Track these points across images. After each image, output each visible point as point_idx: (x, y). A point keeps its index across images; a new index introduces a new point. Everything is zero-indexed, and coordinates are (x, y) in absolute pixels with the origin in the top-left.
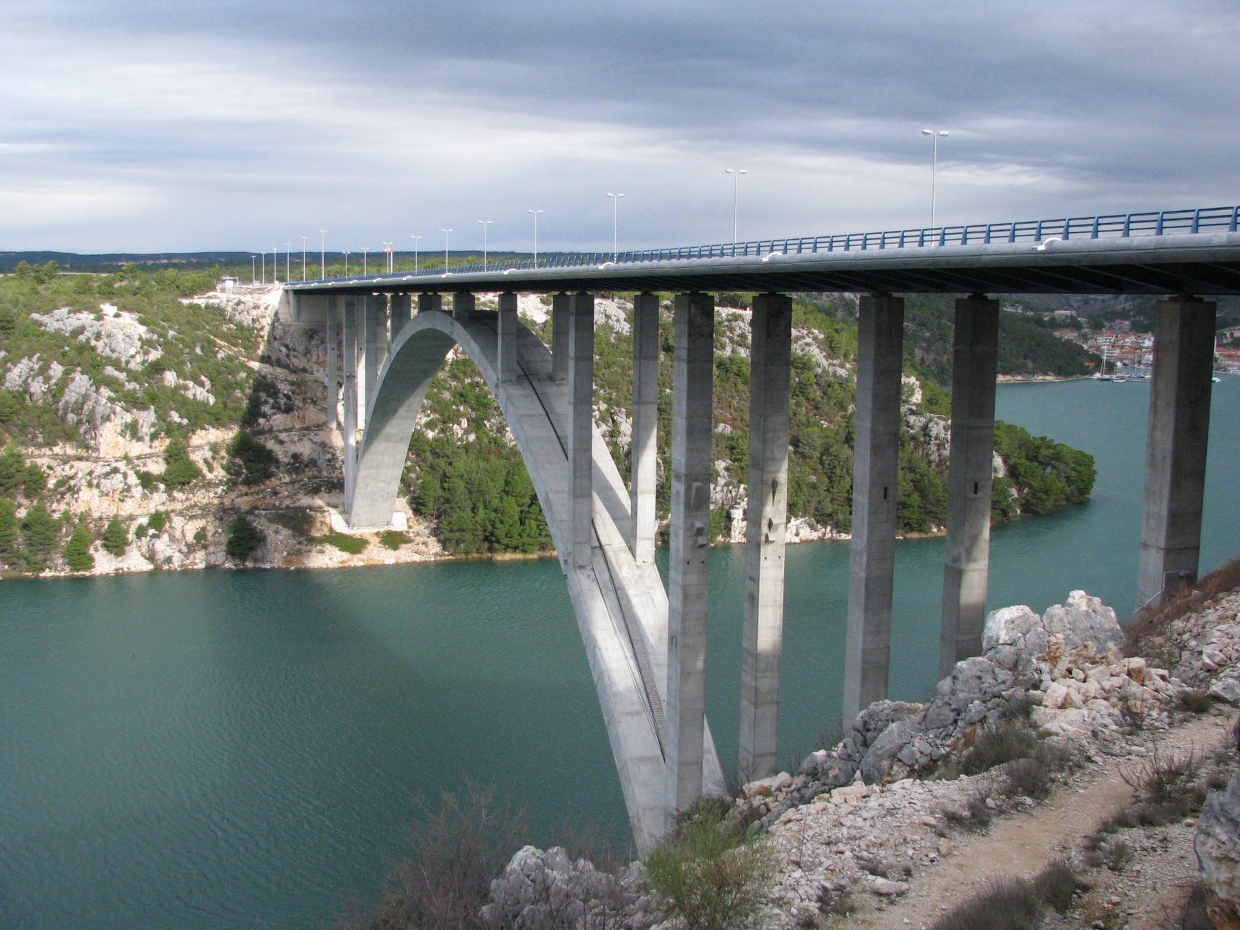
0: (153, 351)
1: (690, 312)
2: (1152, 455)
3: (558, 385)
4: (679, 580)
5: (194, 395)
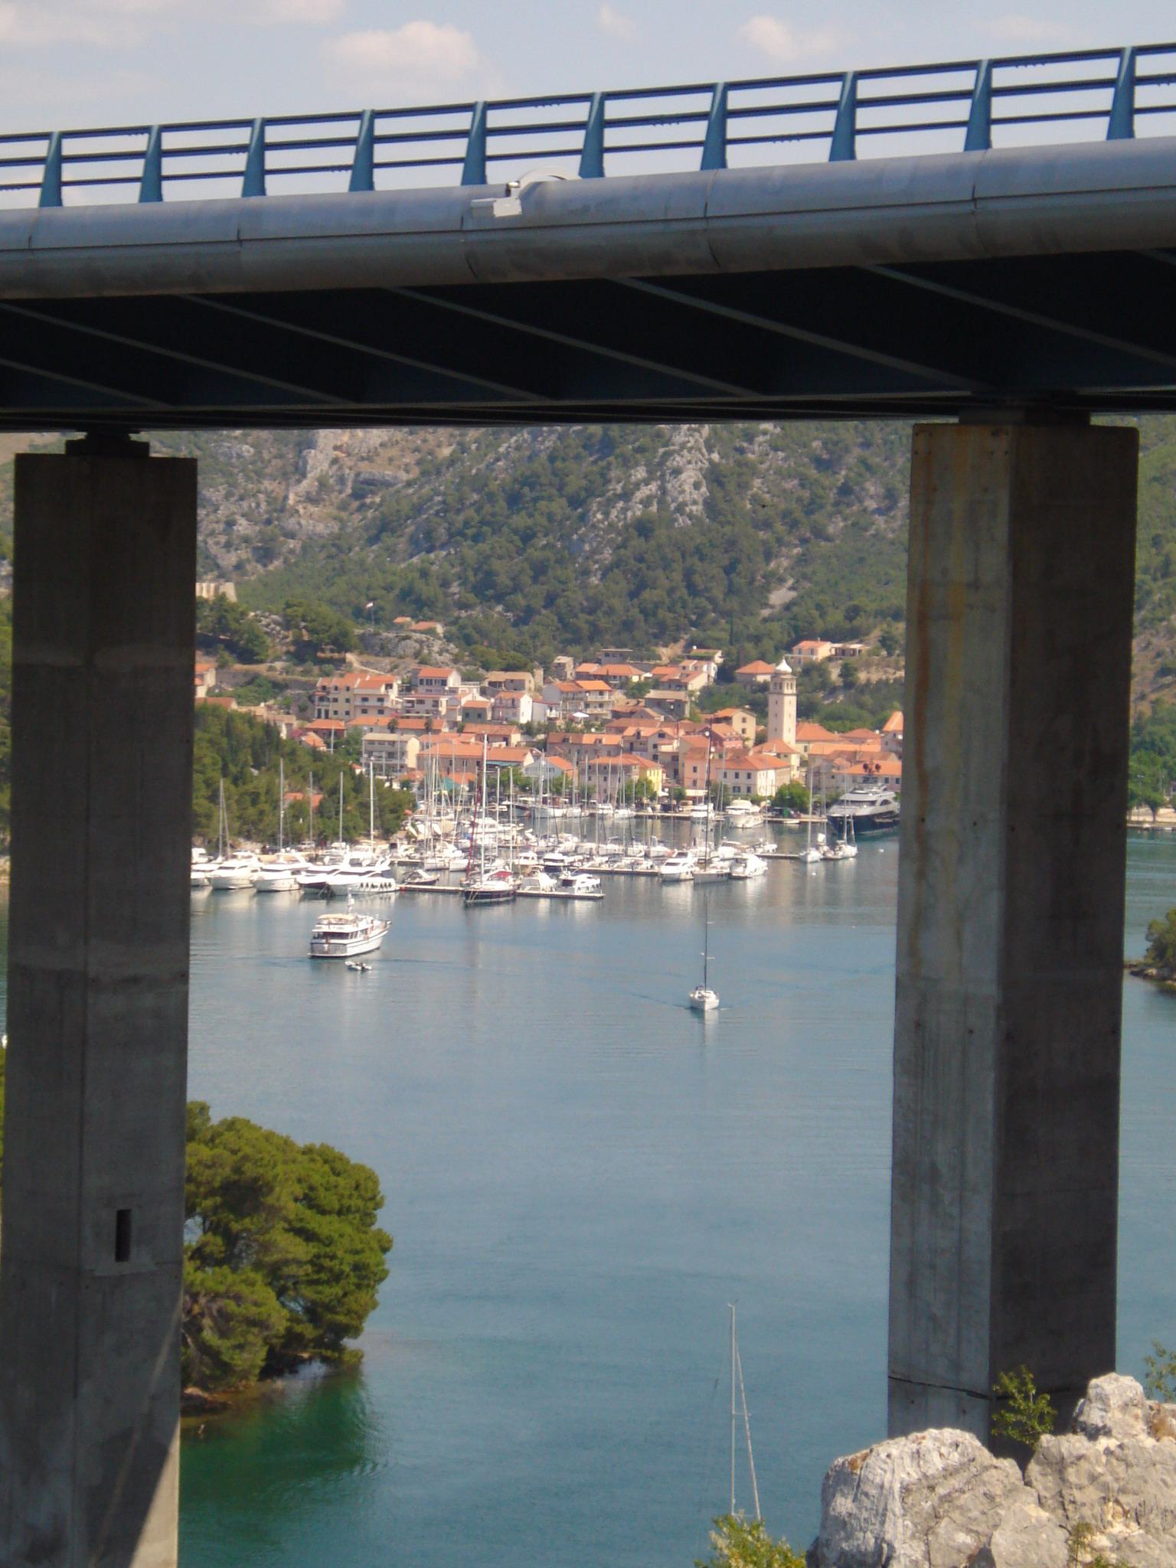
2: (919, 1025)
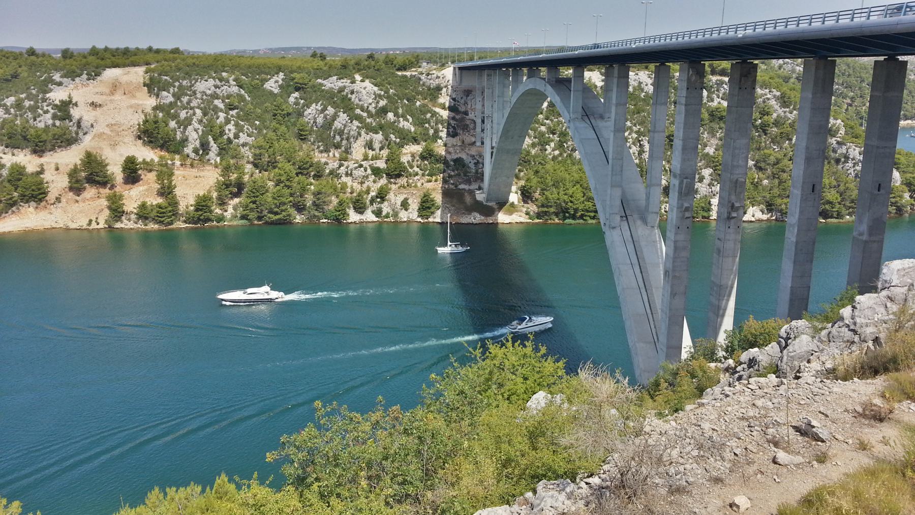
0: (381, 101)
1: (688, 74)
3: (606, 121)
4: (673, 238)
5: (403, 126)
